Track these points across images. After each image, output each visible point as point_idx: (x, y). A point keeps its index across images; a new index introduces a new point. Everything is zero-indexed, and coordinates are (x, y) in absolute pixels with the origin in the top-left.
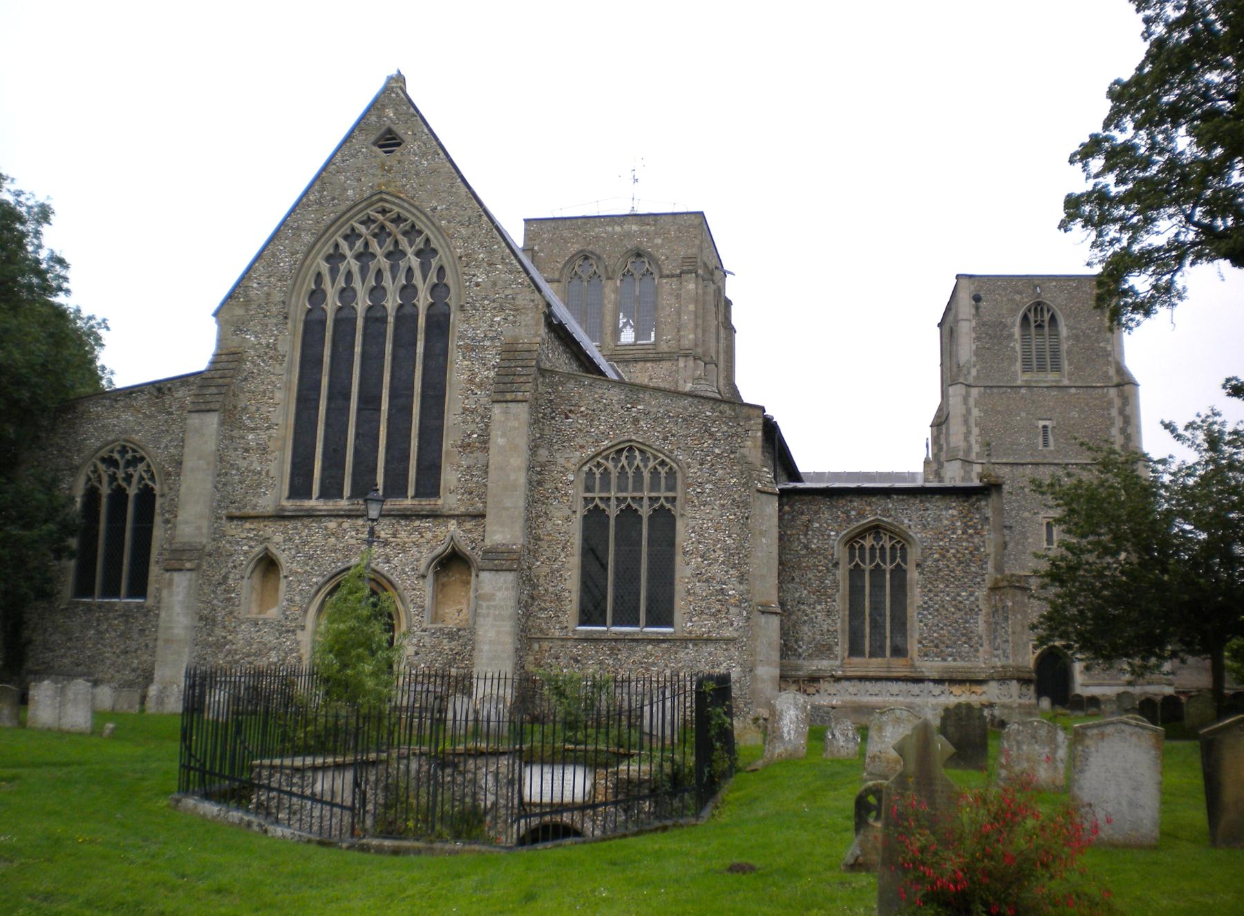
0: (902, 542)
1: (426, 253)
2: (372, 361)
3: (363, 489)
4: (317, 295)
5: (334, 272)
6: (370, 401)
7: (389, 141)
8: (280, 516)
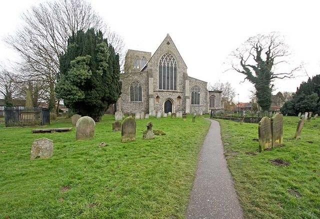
0: (215, 96)
1: (174, 59)
2: (168, 72)
3: (168, 89)
4: (161, 63)
5: (166, 61)
6: (168, 78)
7: (168, 43)
8: (159, 91)
